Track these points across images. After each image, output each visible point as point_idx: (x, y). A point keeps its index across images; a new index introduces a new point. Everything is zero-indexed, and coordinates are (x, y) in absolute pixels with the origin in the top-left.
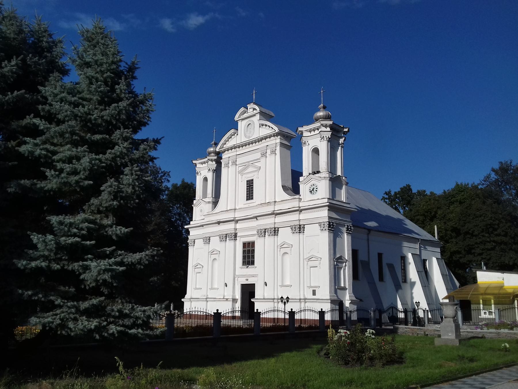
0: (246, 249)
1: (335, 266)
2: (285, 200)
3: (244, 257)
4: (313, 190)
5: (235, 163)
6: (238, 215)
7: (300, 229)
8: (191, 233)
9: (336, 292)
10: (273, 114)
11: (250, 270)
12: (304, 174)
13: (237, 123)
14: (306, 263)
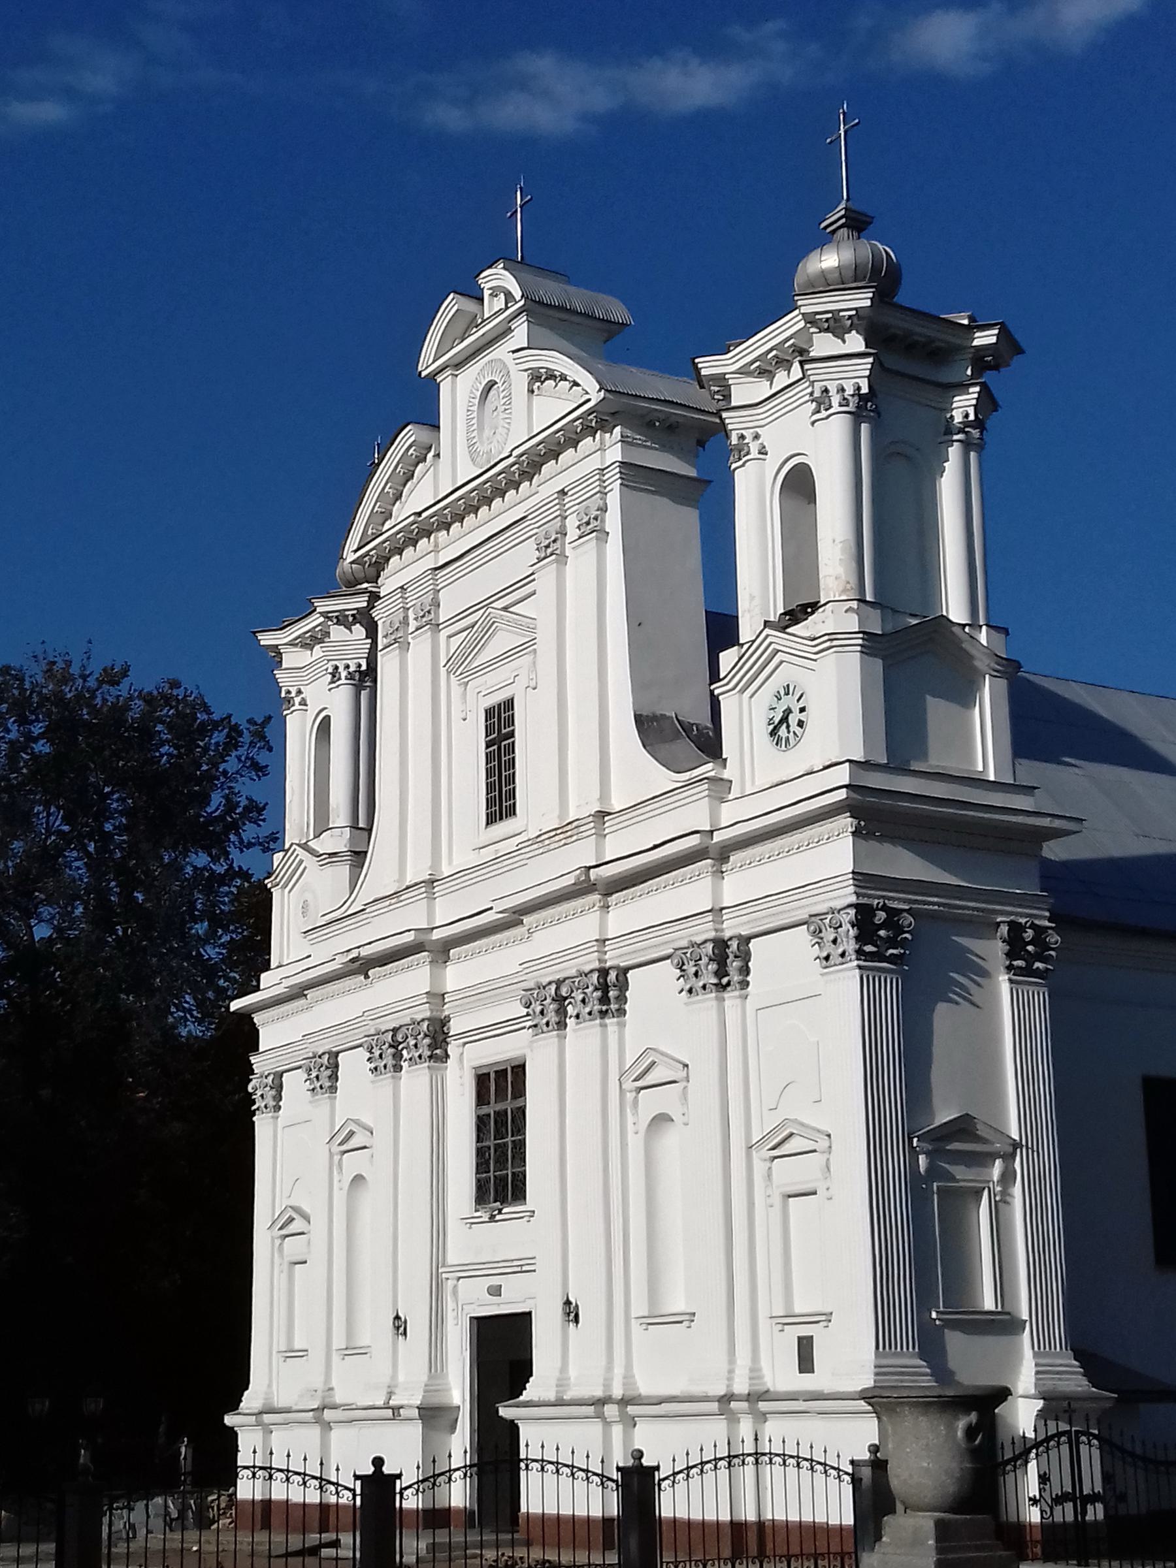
0: (490, 1110)
1: (917, 1187)
2: (654, 803)
4: (785, 719)
6: (446, 913)
7: (723, 963)
8: (267, 1038)
9: (930, 1346)
10: (618, 312)
11: (507, 1235)
12: (745, 635)
13: (431, 386)
14: (759, 1167)
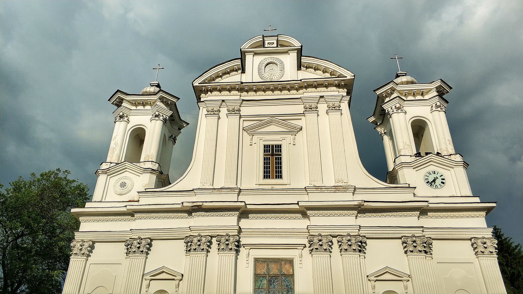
4: (434, 181)
5: (235, 112)
6: (251, 200)
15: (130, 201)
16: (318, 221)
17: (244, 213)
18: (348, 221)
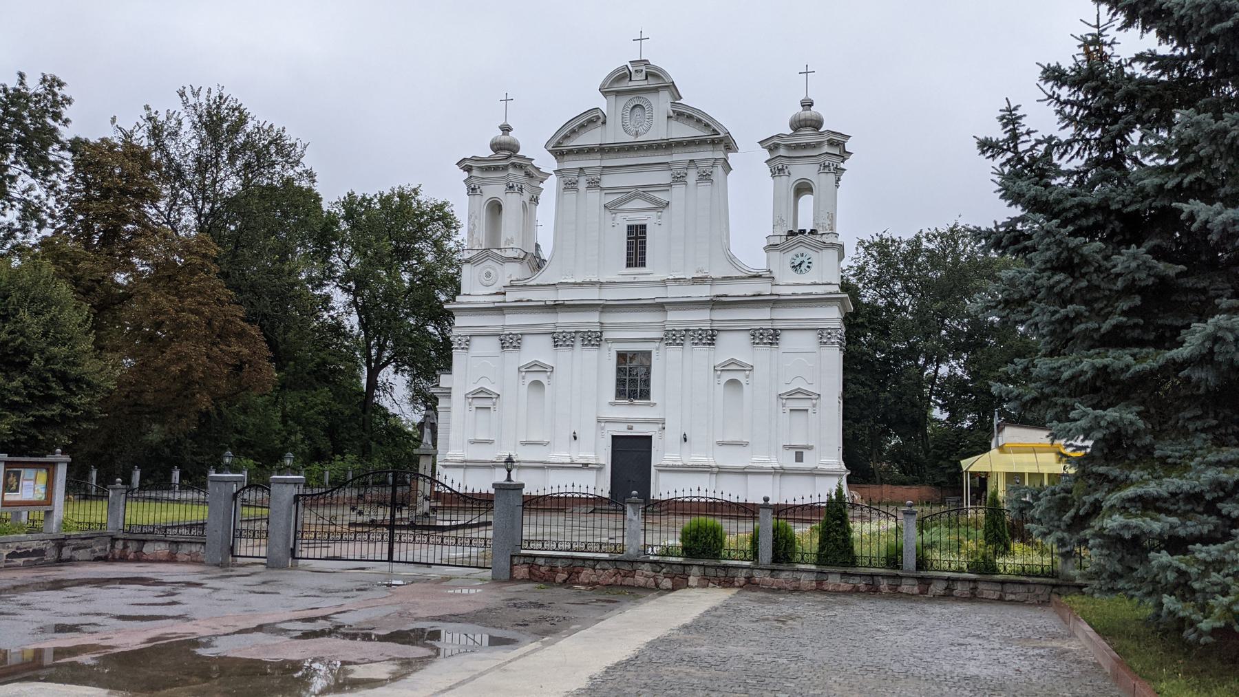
3: (620, 382)
5: (594, 184)
6: (610, 295)
8: (459, 321)
15: (497, 294)
16: (676, 318)
17: (605, 308)
18: (701, 318)
